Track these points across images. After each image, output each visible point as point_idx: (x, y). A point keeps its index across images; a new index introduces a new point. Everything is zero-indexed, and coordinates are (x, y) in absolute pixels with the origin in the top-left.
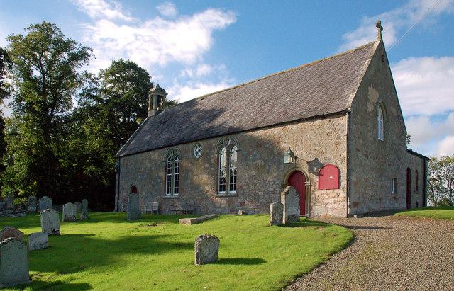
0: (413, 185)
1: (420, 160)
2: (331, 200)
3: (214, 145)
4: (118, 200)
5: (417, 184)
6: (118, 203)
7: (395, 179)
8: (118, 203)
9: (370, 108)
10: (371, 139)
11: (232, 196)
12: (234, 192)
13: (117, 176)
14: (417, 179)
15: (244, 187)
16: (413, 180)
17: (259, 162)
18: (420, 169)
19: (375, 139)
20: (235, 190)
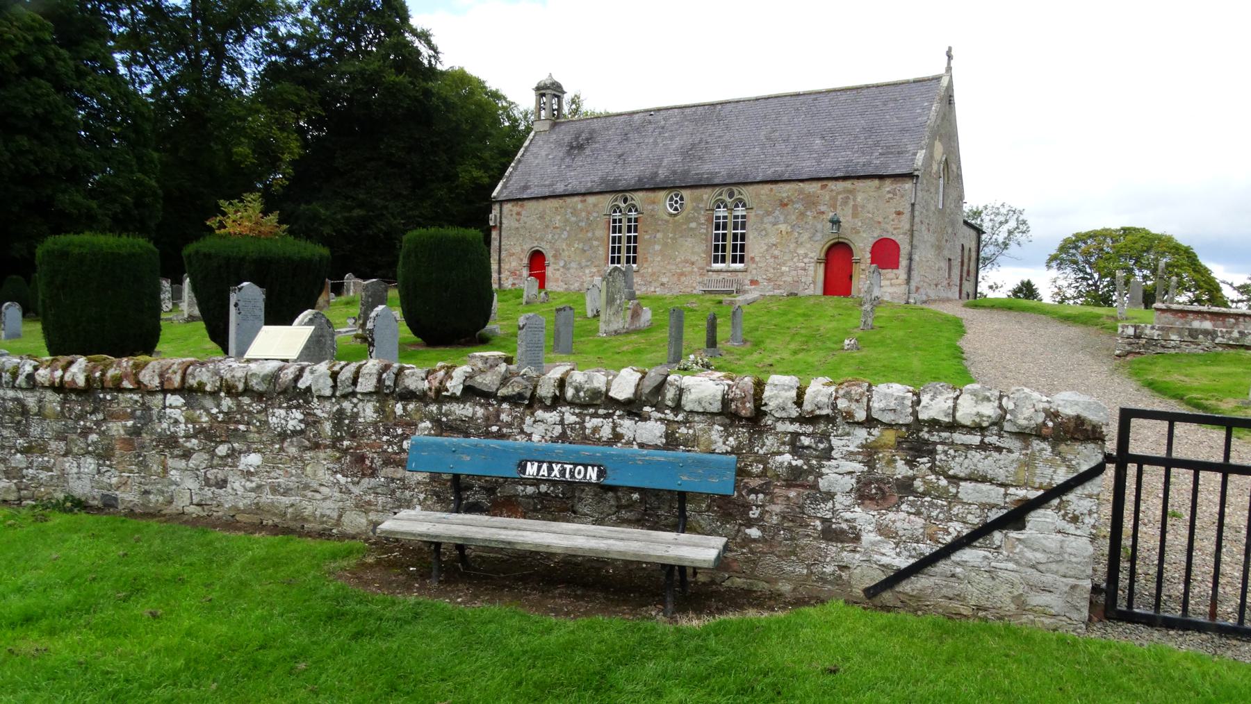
0: (965, 268)
1: (973, 233)
2: (888, 283)
3: (705, 197)
4: (500, 273)
5: (969, 266)
6: (500, 279)
7: (950, 260)
8: (500, 279)
9: (935, 167)
10: (933, 208)
11: (735, 271)
12: (738, 266)
13: (494, 234)
14: (970, 260)
15: (757, 259)
16: (966, 261)
17: (783, 227)
18: (973, 245)
19: (936, 206)
20: (742, 261)
